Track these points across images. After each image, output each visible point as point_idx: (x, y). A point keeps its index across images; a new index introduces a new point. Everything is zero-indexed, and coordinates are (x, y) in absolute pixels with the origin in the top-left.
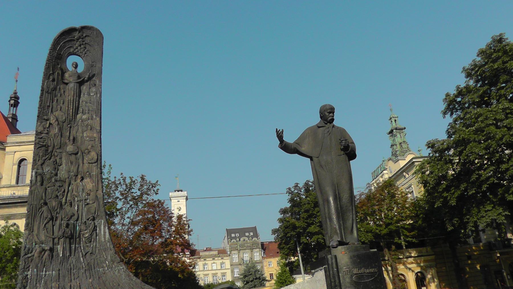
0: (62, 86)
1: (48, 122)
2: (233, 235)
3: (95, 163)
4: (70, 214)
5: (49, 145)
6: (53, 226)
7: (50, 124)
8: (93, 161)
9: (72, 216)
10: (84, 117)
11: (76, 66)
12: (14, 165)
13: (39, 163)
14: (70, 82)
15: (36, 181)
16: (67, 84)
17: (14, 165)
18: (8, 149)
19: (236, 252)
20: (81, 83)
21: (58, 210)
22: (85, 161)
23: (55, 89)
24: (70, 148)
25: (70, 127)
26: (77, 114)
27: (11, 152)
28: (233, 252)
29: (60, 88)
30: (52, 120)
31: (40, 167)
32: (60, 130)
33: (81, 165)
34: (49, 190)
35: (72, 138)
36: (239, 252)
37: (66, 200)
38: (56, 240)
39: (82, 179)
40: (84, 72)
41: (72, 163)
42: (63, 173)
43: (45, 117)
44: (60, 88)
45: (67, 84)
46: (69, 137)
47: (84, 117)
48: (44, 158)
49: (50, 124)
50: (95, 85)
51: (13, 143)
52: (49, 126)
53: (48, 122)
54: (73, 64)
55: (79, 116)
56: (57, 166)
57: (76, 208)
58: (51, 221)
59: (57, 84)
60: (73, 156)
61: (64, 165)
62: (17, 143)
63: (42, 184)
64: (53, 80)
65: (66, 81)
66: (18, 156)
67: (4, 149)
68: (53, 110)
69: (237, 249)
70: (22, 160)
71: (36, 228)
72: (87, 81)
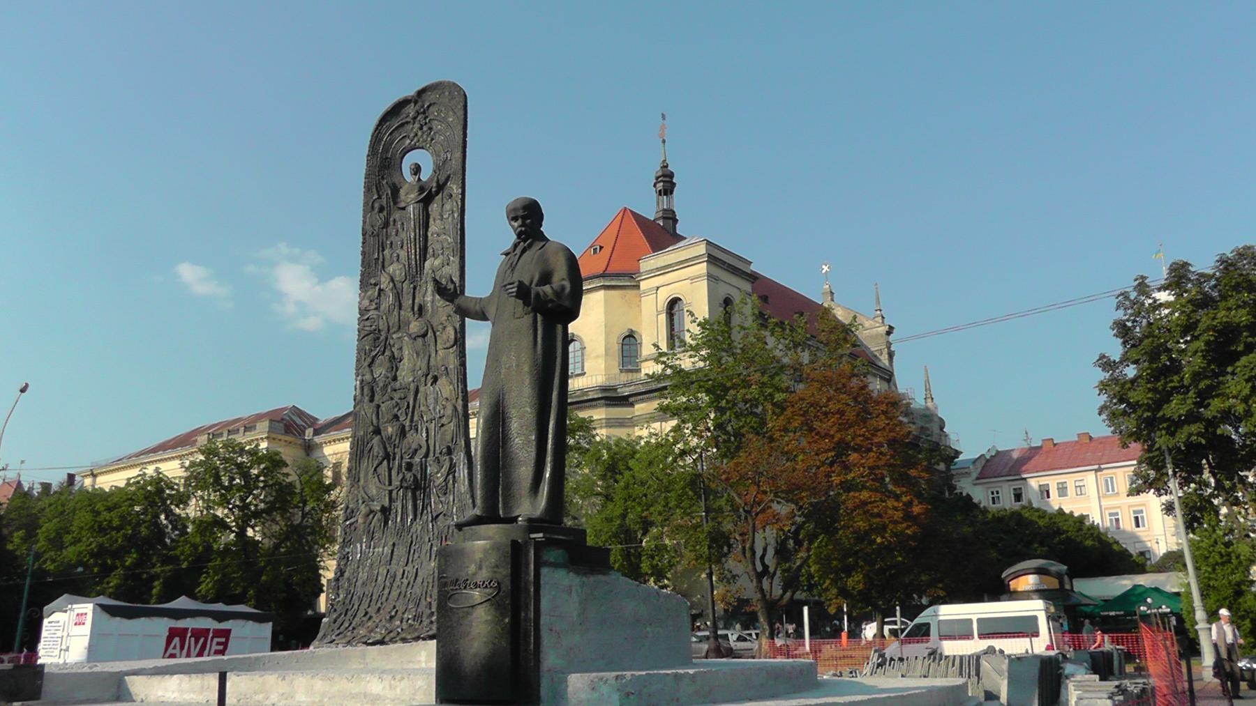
4: (414, 446)
6: (390, 470)
7: (380, 290)
8: (448, 345)
9: (416, 451)
10: (437, 262)
11: (417, 170)
12: (658, 313)
13: (366, 364)
14: (408, 204)
15: (362, 394)
17: (658, 313)
18: (644, 285)
22: (439, 346)
23: (386, 224)
24: (415, 327)
25: (415, 288)
27: (650, 289)
30: (385, 282)
32: (398, 297)
33: (433, 355)
34: (383, 407)
35: (416, 308)
39: (435, 379)
40: (431, 179)
41: (418, 354)
42: (405, 375)
43: (373, 281)
45: (404, 209)
46: (413, 308)
47: (437, 262)
49: (380, 290)
51: (651, 271)
52: (379, 295)
55: (427, 264)
56: (394, 362)
57: (424, 435)
59: (389, 214)
60: (420, 340)
61: (406, 360)
62: (658, 269)
63: (372, 400)
64: (381, 209)
65: (402, 205)
66: (664, 296)
67: (638, 287)
68: (386, 264)
70: (673, 303)
71: (362, 475)
72: (437, 193)
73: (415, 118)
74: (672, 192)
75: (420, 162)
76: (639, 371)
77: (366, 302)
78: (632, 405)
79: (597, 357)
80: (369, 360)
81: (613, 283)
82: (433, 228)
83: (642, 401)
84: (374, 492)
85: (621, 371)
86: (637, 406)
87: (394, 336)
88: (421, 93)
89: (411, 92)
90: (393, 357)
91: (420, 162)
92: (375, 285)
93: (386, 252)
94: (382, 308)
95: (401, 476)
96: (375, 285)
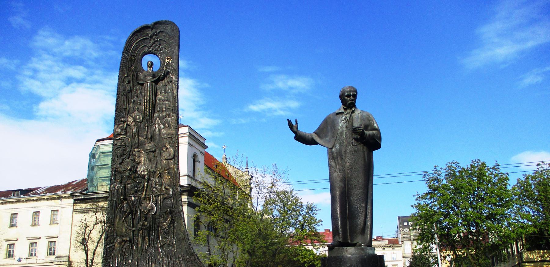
0: (138, 87)
1: (125, 124)
3: (172, 159)
5: (127, 145)
6: (133, 219)
7: (127, 125)
11: (151, 65)
13: (118, 163)
14: (146, 82)
16: (142, 85)
19: (409, 242)
20: (156, 82)
21: (137, 205)
22: (163, 158)
23: (131, 91)
26: (154, 113)
28: (405, 242)
29: (136, 90)
37: (145, 194)
38: (136, 233)
41: (150, 161)
44: (136, 90)
45: (142, 85)
46: (147, 137)
48: (123, 158)
49: (127, 125)
50: (171, 82)
52: (127, 127)
53: (125, 124)
54: (148, 63)
55: (156, 115)
59: (134, 86)
64: (129, 82)
65: (141, 82)
68: (131, 111)
69: (410, 240)
72: (163, 79)
73: (151, 37)
75: (150, 62)
77: (119, 130)
80: (120, 160)
82: (160, 96)
84: (124, 230)
87: (136, 150)
88: (156, 24)
90: (134, 160)
92: (124, 122)
93: (131, 105)
94: (128, 135)
95: (141, 223)
96: (124, 122)
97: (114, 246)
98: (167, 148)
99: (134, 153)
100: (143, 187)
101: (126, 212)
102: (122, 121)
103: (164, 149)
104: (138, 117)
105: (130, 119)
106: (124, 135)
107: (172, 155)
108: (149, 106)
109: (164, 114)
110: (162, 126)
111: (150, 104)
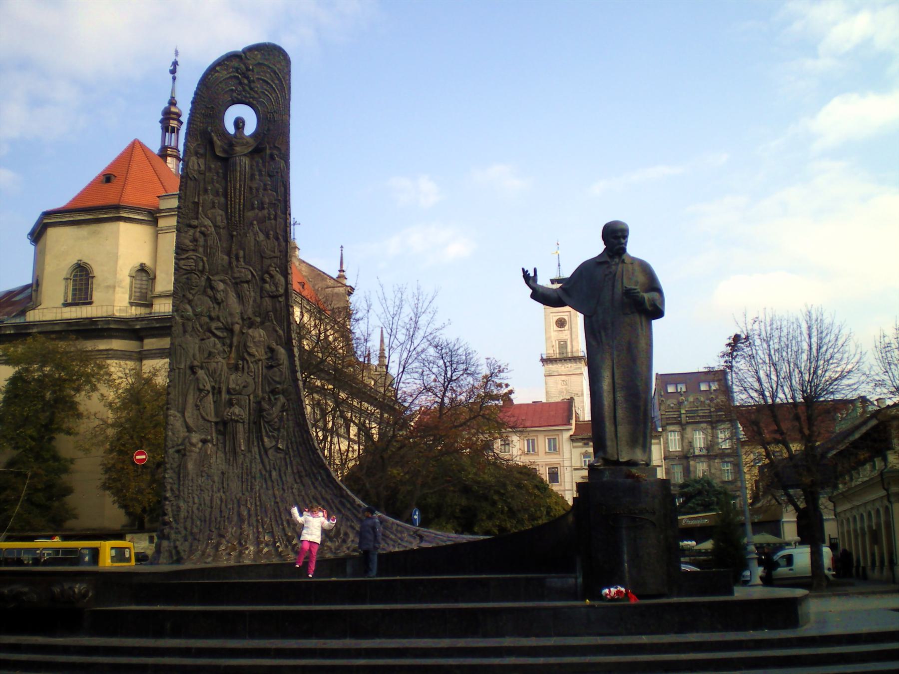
2: (671, 389)
3: (281, 296)
9: (244, 387)
11: (239, 123)
31: (188, 307)
36: (684, 429)
49: (202, 233)
58: (211, 395)
60: (246, 285)
74: (178, 130)
76: (150, 305)
77: (187, 242)
78: (141, 339)
79: (108, 287)
81: (131, 216)
83: (153, 336)
85: (131, 304)
86: (146, 341)
87: (216, 278)
89: (239, 48)
91: (242, 117)
92: (195, 227)
97: (185, 449)
98: (272, 277)
99: (214, 284)
100: (231, 346)
101: (200, 390)
102: (190, 226)
103: (266, 276)
104: (219, 218)
105: (208, 222)
106: (193, 250)
107: (281, 291)
108: (240, 200)
109: (266, 212)
110: (261, 237)
111: (240, 196)
